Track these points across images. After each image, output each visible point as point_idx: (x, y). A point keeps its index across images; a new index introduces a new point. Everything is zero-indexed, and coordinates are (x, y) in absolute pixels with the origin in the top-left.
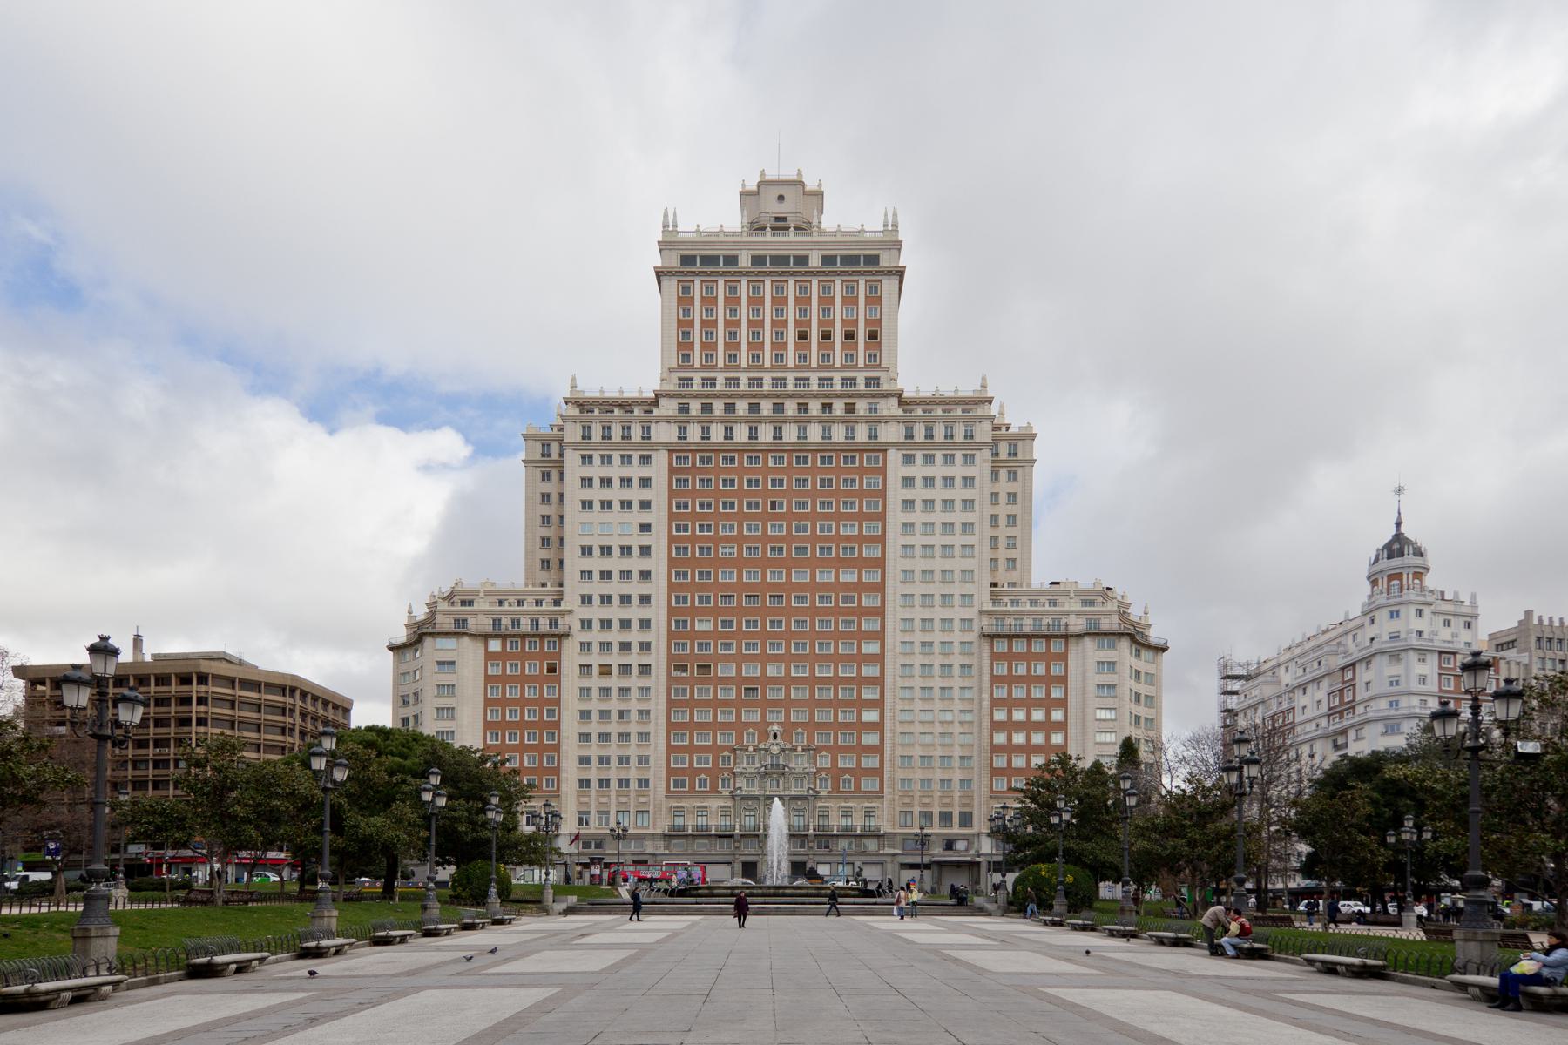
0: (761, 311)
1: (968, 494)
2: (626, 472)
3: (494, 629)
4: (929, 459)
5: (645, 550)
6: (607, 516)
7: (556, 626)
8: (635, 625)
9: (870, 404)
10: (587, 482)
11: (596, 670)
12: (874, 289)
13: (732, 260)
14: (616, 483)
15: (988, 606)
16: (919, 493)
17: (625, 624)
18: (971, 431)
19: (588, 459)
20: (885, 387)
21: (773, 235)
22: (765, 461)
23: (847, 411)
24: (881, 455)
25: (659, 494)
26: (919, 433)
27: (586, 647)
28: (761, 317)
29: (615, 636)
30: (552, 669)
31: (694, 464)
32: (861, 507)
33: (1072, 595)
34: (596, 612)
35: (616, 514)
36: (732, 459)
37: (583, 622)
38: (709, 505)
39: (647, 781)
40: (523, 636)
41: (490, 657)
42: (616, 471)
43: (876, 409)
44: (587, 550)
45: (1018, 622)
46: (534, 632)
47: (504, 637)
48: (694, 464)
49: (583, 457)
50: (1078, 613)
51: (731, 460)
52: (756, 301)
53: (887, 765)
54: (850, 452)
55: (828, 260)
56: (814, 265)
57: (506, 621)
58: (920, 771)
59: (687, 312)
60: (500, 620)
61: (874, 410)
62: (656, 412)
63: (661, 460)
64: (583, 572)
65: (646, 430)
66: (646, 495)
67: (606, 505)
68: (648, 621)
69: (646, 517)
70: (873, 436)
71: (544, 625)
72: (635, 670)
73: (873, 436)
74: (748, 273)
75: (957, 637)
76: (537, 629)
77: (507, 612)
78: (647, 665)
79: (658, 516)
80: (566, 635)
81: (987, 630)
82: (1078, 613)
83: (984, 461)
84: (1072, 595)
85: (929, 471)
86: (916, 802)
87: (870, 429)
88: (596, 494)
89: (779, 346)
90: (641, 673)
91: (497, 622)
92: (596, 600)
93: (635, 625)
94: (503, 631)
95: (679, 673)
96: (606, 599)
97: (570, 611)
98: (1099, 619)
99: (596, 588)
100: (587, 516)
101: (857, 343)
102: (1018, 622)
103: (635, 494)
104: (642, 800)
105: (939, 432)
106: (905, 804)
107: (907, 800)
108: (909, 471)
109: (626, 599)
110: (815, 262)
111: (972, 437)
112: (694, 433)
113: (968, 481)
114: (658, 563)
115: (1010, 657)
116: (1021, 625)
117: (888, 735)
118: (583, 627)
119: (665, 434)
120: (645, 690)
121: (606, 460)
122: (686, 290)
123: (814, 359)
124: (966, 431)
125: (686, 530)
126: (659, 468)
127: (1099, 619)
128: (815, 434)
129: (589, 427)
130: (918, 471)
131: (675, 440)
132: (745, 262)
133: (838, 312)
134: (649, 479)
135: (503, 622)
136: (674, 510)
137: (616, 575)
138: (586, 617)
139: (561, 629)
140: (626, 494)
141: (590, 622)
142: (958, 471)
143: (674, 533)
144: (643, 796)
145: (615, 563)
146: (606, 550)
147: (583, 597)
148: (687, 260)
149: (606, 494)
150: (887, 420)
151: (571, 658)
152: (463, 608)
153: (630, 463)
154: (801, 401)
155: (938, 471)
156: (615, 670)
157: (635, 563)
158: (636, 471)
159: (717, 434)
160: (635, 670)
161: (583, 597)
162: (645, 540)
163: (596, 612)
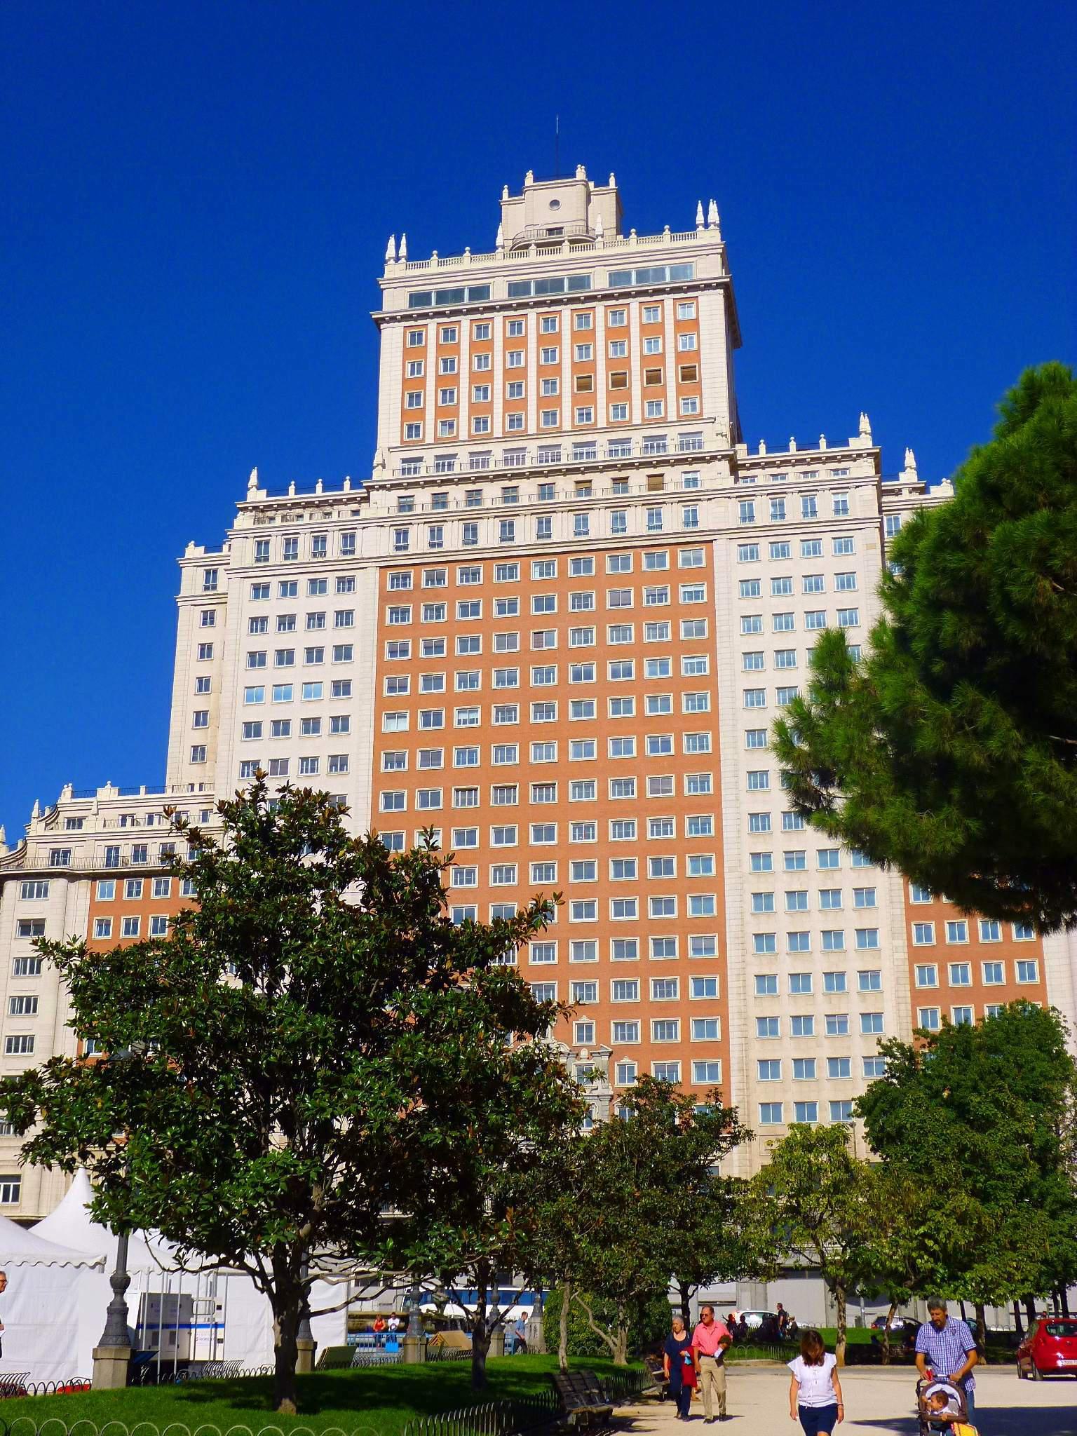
0: (523, 355)
2: (318, 604)
3: (108, 865)
4: (781, 551)
5: (341, 724)
6: (285, 674)
10: (258, 624)
13: (480, 292)
19: (261, 591)
21: (538, 253)
22: (526, 573)
23: (651, 487)
26: (763, 510)
28: (523, 364)
31: (417, 585)
32: (676, 633)
35: (299, 672)
36: (475, 574)
38: (439, 648)
40: (148, 875)
41: (94, 907)
42: (301, 605)
43: (695, 480)
44: (252, 730)
48: (417, 585)
49: (256, 588)
51: (474, 574)
52: (515, 344)
53: (735, 1078)
54: (654, 547)
56: (597, 287)
57: (126, 851)
58: (794, 1087)
59: (416, 367)
60: (117, 849)
63: (368, 582)
65: (349, 539)
66: (344, 636)
67: (285, 657)
69: (342, 671)
74: (504, 308)
79: (361, 671)
83: (870, 547)
85: (781, 568)
88: (271, 641)
91: (112, 853)
94: (121, 869)
100: (257, 676)
101: (665, 385)
103: (328, 637)
105: (794, 506)
108: (750, 570)
111: (845, 511)
112: (419, 539)
117: (734, 1021)
121: (289, 589)
122: (417, 337)
123: (602, 415)
124: (837, 502)
125: (403, 688)
128: (600, 525)
130: (765, 569)
132: (499, 293)
134: (350, 613)
135: (121, 853)
142: (828, 563)
143: (386, 693)
146: (282, 728)
148: (418, 299)
149: (286, 640)
150: (711, 495)
152: (71, 831)
153: (323, 590)
154: (580, 477)
158: (330, 602)
159: (453, 536)
162: (341, 707)
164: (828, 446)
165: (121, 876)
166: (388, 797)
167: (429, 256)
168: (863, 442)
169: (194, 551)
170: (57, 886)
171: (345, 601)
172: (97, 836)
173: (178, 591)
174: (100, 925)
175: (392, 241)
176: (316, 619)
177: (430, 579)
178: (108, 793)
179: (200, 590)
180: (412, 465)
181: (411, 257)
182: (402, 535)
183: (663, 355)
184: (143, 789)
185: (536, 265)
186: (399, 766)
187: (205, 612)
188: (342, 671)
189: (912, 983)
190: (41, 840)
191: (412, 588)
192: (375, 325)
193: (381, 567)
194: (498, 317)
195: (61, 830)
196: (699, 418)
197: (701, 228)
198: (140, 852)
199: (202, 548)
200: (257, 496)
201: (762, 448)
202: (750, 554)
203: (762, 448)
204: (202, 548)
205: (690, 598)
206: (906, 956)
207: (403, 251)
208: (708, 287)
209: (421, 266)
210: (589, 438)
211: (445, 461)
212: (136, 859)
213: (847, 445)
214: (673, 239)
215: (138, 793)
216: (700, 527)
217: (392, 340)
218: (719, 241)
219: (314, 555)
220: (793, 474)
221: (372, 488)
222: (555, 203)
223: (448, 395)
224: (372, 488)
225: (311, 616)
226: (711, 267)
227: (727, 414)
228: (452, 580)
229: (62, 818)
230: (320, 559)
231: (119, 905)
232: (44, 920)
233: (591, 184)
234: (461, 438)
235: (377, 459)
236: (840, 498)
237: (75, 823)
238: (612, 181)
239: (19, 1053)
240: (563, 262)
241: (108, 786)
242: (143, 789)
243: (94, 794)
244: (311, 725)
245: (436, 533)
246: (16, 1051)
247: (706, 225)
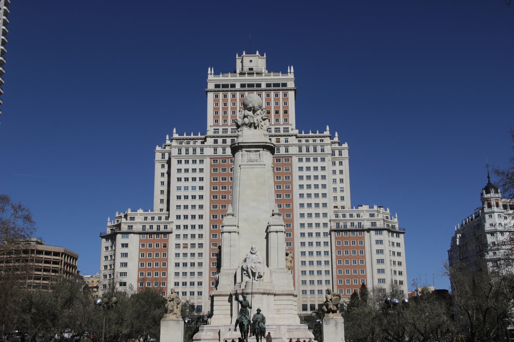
1: (323, 173)
2: (194, 166)
4: (308, 160)
5: (201, 197)
6: (187, 184)
7: (167, 228)
8: (197, 227)
9: (285, 138)
10: (179, 170)
11: (182, 246)
13: (233, 86)
14: (190, 170)
15: (333, 218)
16: (305, 173)
17: (193, 227)
18: (323, 149)
19: (180, 162)
20: (291, 132)
21: (248, 76)
24: (290, 158)
25: (206, 175)
27: (178, 236)
29: (189, 232)
30: (165, 246)
31: (220, 163)
33: (365, 213)
34: (182, 222)
35: (190, 184)
37: (177, 226)
39: (201, 292)
40: (154, 233)
41: (141, 241)
42: (190, 166)
45: (345, 224)
46: (158, 231)
47: (147, 233)
48: (220, 163)
49: (178, 161)
50: (368, 220)
55: (268, 85)
57: (148, 227)
60: (145, 226)
61: (287, 141)
62: (206, 144)
63: (207, 162)
64: (177, 206)
65: (202, 150)
67: (187, 179)
68: (202, 226)
69: (201, 184)
70: (287, 151)
71: (162, 229)
72: (197, 246)
73: (287, 151)
74: (239, 91)
75: (322, 230)
76: (159, 230)
77: (148, 223)
78: (201, 244)
79: (206, 184)
80: (171, 233)
81: (334, 227)
82: (368, 220)
84: (365, 213)
85: (308, 164)
86: (309, 300)
87: (286, 149)
88: (183, 175)
90: (199, 247)
91: (144, 227)
92: (182, 217)
93: (197, 227)
95: (214, 247)
96: (186, 217)
97: (172, 222)
98: (376, 222)
99: (182, 212)
100: (179, 184)
102: (345, 224)
103: (198, 175)
104: (199, 301)
105: (311, 149)
106: (304, 301)
107: (305, 299)
108: (301, 164)
109: (194, 217)
110: (264, 86)
111: (323, 151)
112: (220, 151)
113: (323, 168)
114: (206, 202)
115: (342, 238)
116: (346, 225)
118: (177, 228)
119: (209, 151)
120: (200, 255)
121: (187, 162)
122: (217, 96)
124: (321, 149)
126: (207, 165)
127: (376, 222)
129: (181, 150)
130: (304, 164)
131: (213, 154)
134: (203, 169)
136: (212, 181)
137: (190, 207)
138: (178, 224)
139: (168, 230)
140: (194, 175)
141: (180, 226)
142: (319, 164)
144: (200, 299)
145: (190, 202)
146: (186, 197)
147: (177, 216)
148: (217, 86)
149: (186, 175)
150: (292, 145)
151: (172, 240)
152: (131, 221)
155: (312, 164)
156: (189, 246)
157: (197, 202)
158: (198, 166)
160: (197, 246)
161: (177, 216)
162: (201, 193)
163: (182, 222)
164: (319, 133)
165: (147, 233)
166: (213, 216)
167: (219, 74)
168: (327, 133)
169: (158, 148)
170: (131, 236)
171: (201, 166)
172: (140, 223)
173: (155, 159)
174: (142, 245)
176: (194, 170)
177: (223, 162)
178: (140, 211)
179: (160, 159)
180: (216, 131)
181: (214, 74)
182: (215, 150)
183: (279, 107)
184: (150, 211)
185: (247, 79)
186: (216, 208)
187: (162, 165)
188: (201, 184)
189: (337, 264)
190: (125, 223)
191: (218, 163)
192: (205, 93)
193: (210, 158)
194: (238, 93)
195: (129, 221)
196: (288, 124)
197: (289, 73)
198: (151, 227)
199: (161, 148)
200: (176, 136)
201: (303, 132)
202: (300, 160)
203: (303, 132)
204: (161, 148)
205: (286, 171)
206: (335, 258)
207: (213, 72)
208: (291, 90)
209: (218, 77)
211: (225, 131)
212: (150, 229)
213: (323, 133)
214: (282, 75)
215: (148, 211)
216: (289, 153)
217: (211, 96)
218: (293, 78)
219: (193, 154)
220: (311, 140)
221: (207, 137)
222: (251, 61)
223: (225, 113)
224: (207, 137)
225: (193, 169)
226: (291, 85)
227: (295, 123)
229: (128, 218)
230: (194, 155)
231: (147, 240)
232: (128, 244)
233: (260, 55)
234: (229, 125)
235: (207, 130)
236: (322, 148)
237: (132, 219)
238: (265, 55)
239: (123, 277)
240: (254, 79)
241: (140, 209)
242: (150, 211)
243: (137, 211)
244: (194, 197)
246: (122, 276)
247: (290, 73)
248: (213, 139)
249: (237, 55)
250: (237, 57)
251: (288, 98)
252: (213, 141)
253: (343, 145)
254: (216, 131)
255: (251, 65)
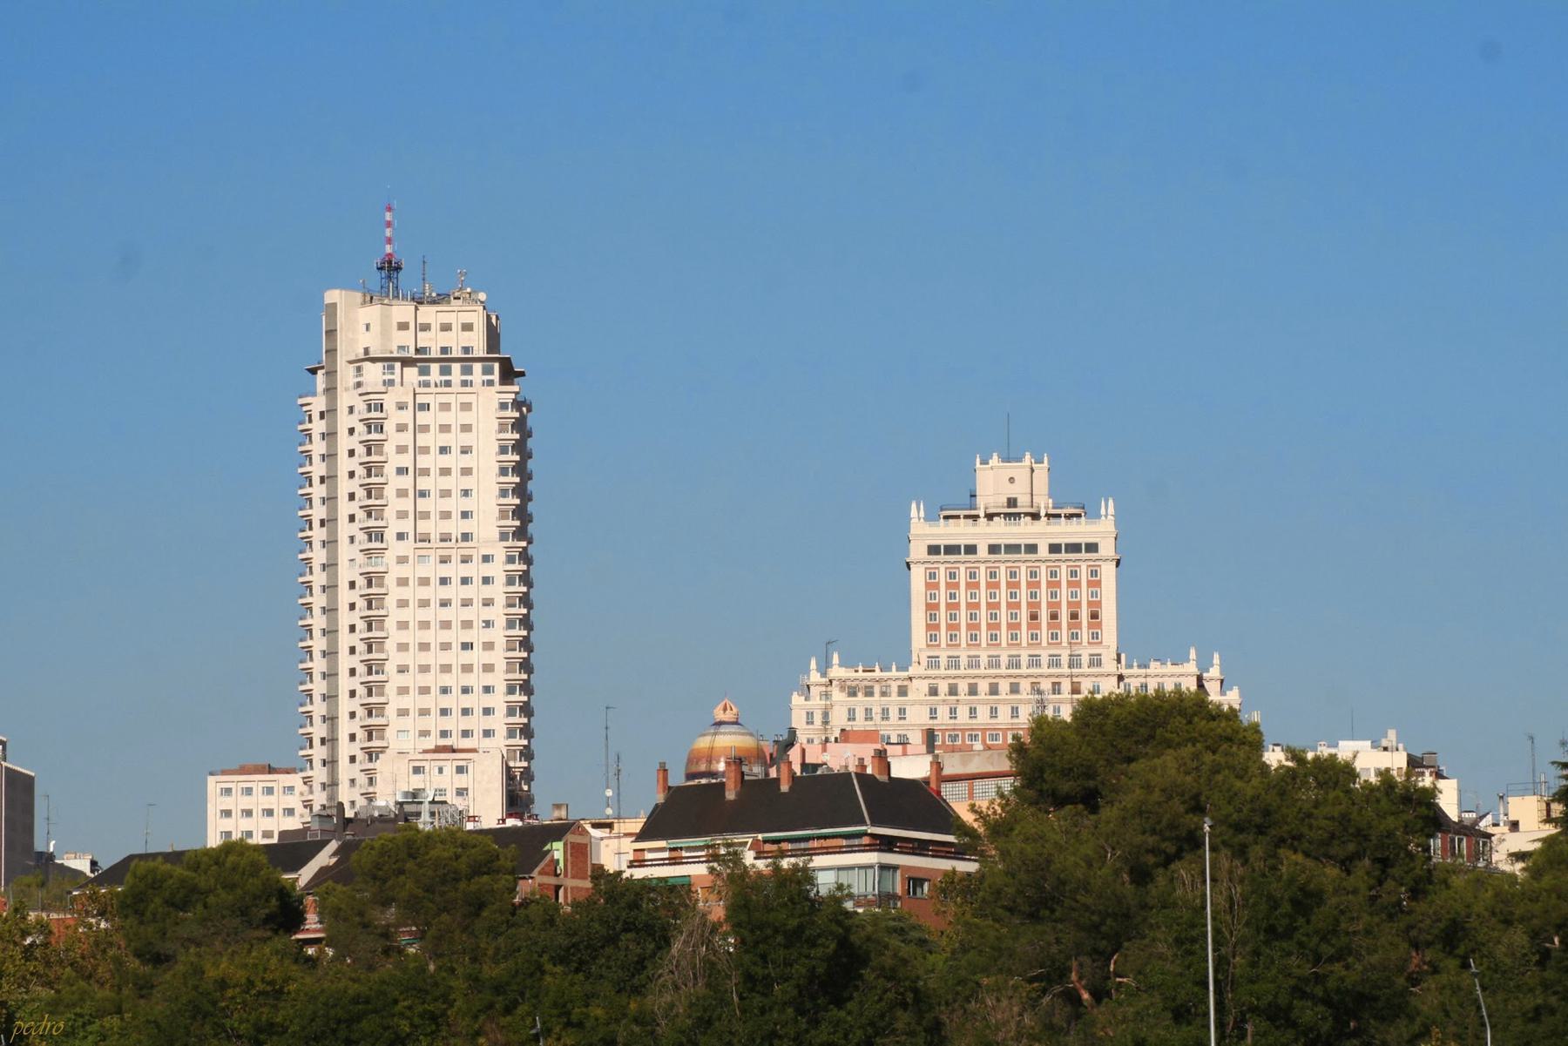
12: (1094, 573)
28: (997, 600)
55: (1054, 548)
59: (933, 596)
65: (902, 711)
89: (1014, 626)
122: (932, 576)
133: (1064, 594)
148: (934, 550)
175: (914, 506)
181: (926, 519)
182: (933, 713)
197: (1103, 518)
204: (803, 698)
207: (922, 514)
210: (1037, 652)
217: (918, 576)
222: (1012, 480)
226: (1107, 549)
228: (963, 740)
235: (915, 658)
238: (1046, 458)
240: (1024, 531)
245: (953, 711)
248: (927, 682)
249: (978, 460)
250: (978, 465)
251: (1100, 581)
252: (926, 690)
253: (1228, 693)
254: (933, 662)
255: (1013, 491)
